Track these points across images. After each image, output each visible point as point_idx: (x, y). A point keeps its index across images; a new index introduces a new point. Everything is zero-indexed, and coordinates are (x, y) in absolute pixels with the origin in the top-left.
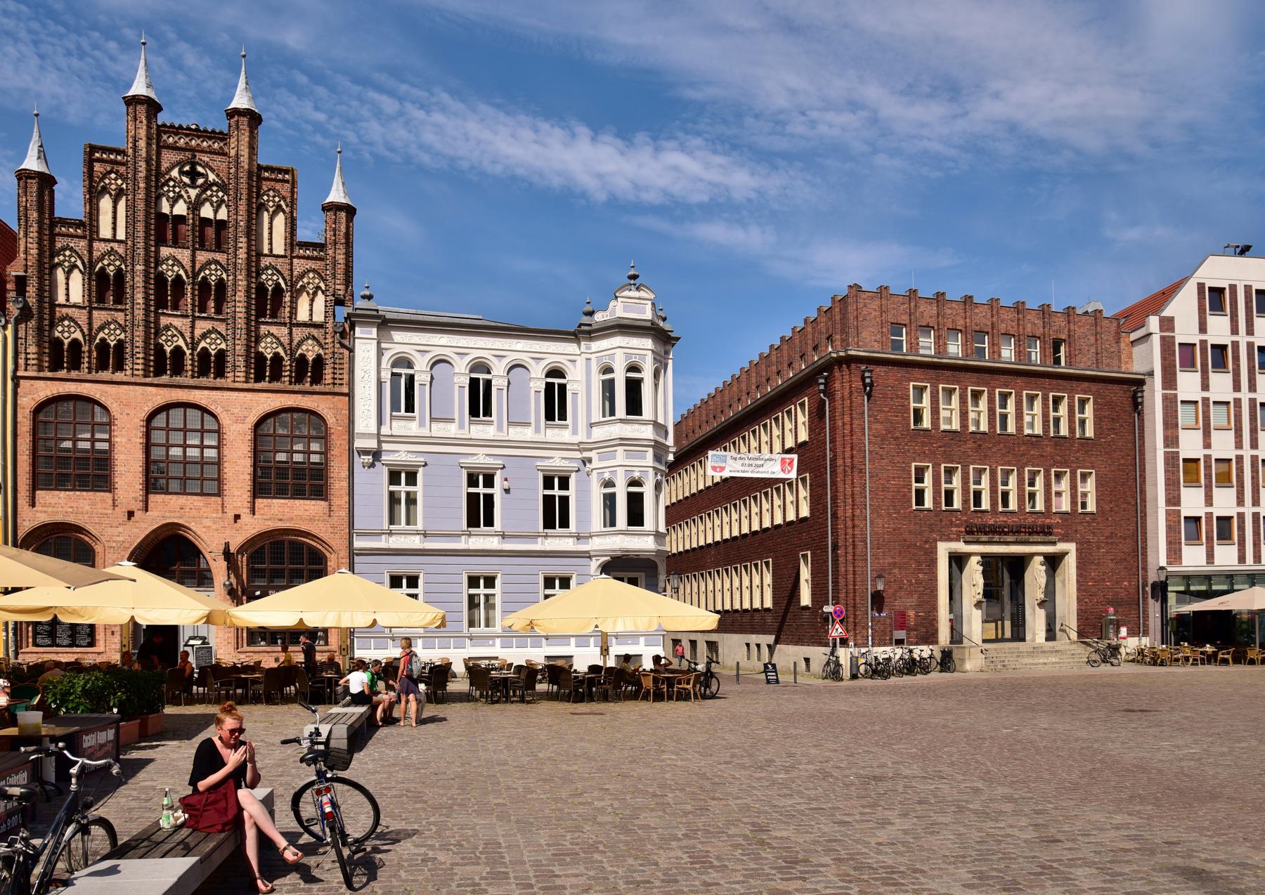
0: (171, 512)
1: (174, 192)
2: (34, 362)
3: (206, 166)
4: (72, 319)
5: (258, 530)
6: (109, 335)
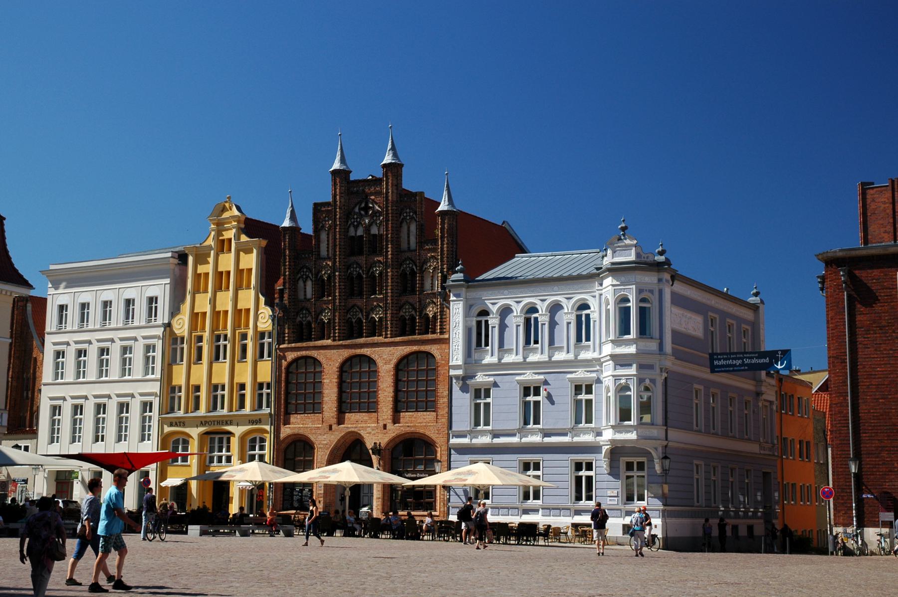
1: (357, 221)
3: (374, 202)
4: (307, 309)
5: (396, 433)
6: (325, 316)
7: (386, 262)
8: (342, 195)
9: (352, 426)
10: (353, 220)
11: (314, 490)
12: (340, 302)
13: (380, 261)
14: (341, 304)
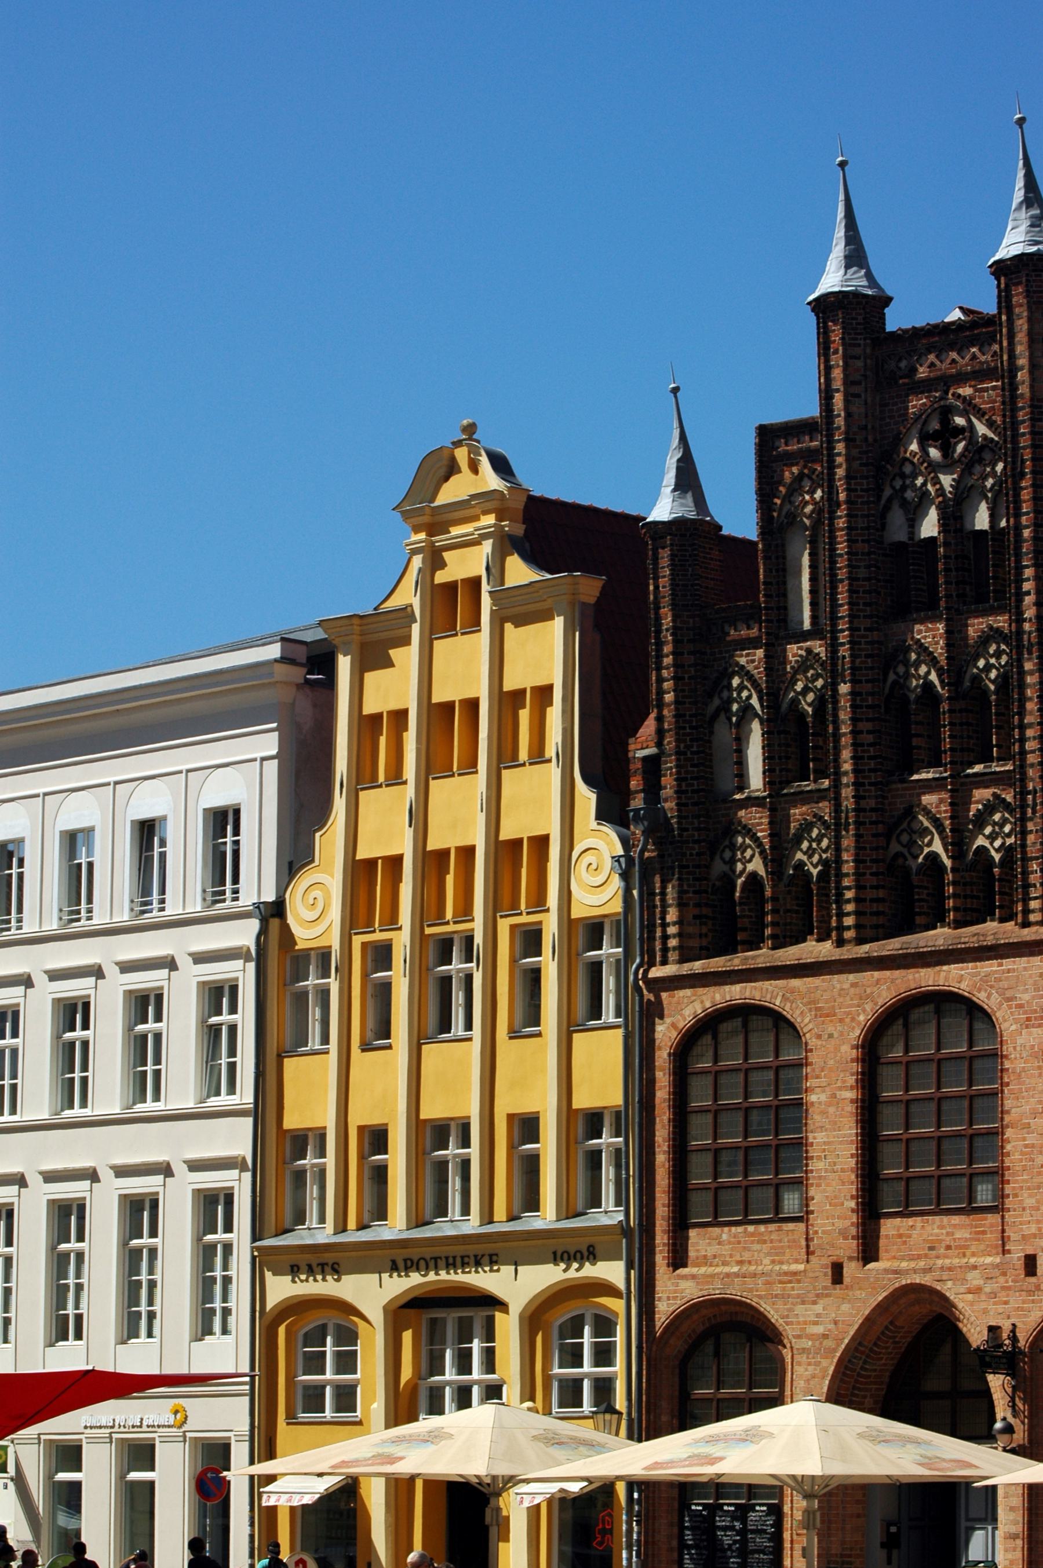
0: (912, 1258)
7: (1020, 632)
8: (855, 389)
9: (912, 1265)
10: (898, 484)
11: (786, 1509)
12: (857, 797)
13: (999, 631)
14: (863, 803)
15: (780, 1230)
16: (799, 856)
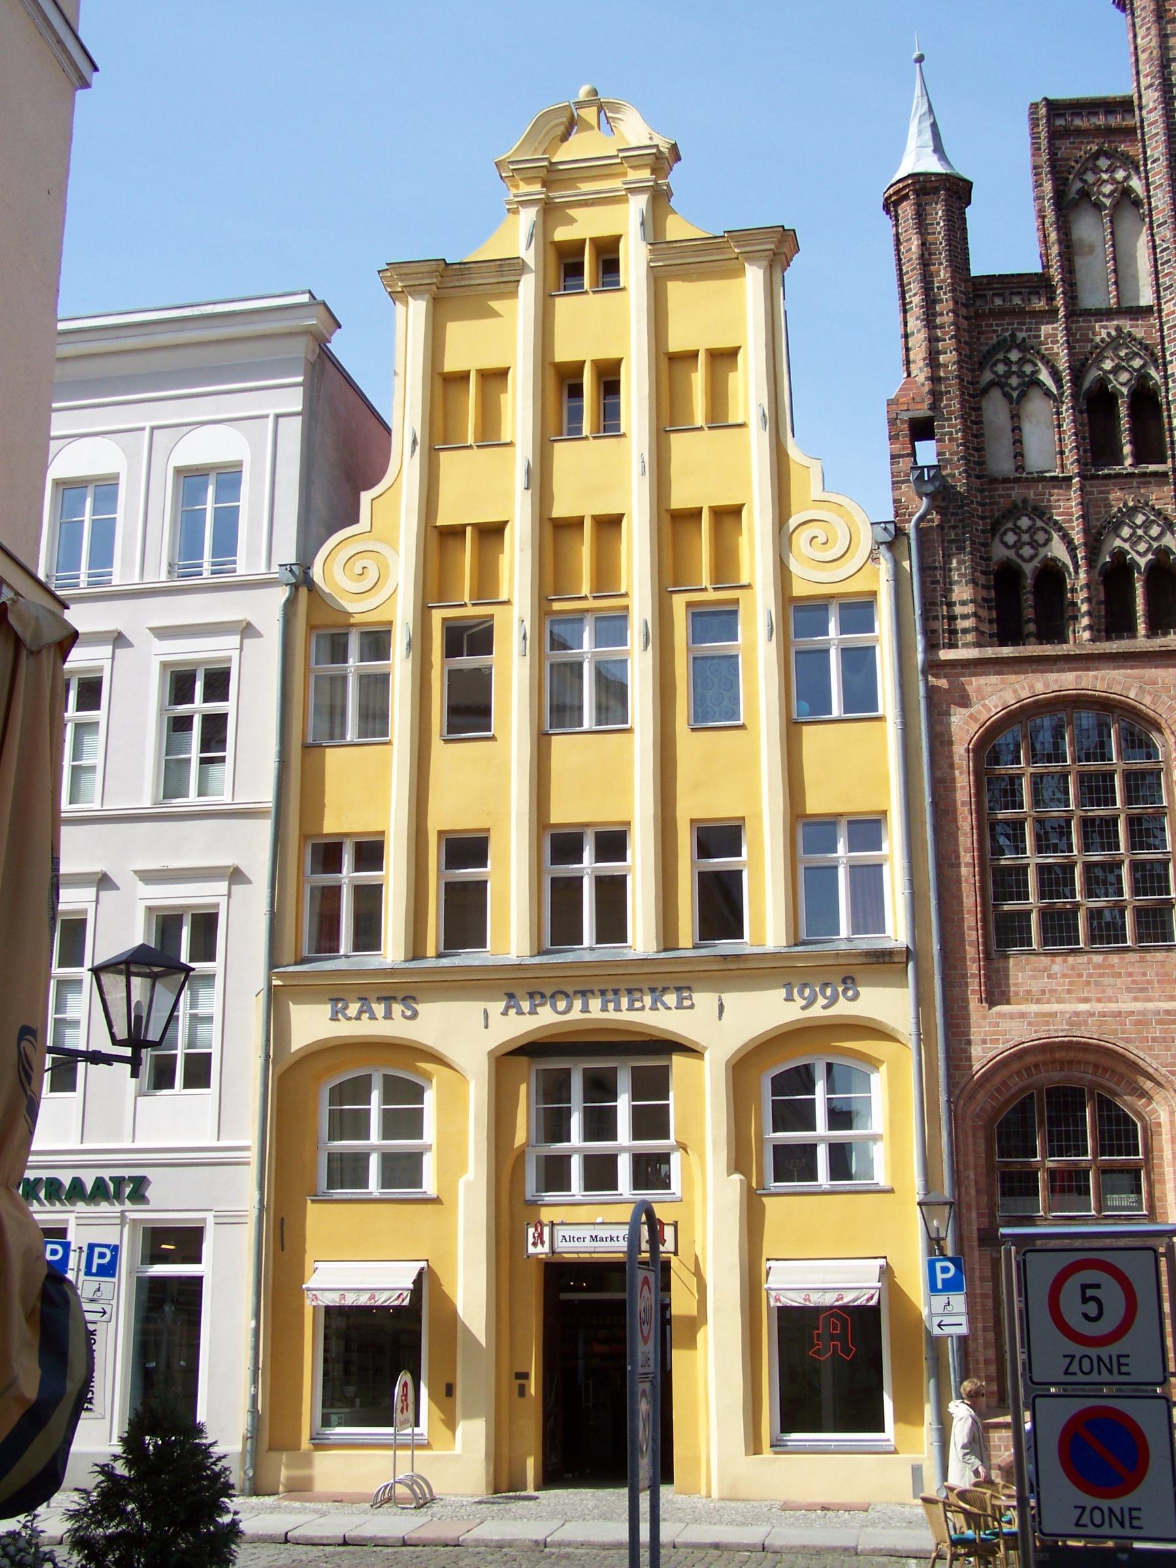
2: (968, 623)
6: (1134, 540)
15: (1142, 960)
16: (1118, 543)
